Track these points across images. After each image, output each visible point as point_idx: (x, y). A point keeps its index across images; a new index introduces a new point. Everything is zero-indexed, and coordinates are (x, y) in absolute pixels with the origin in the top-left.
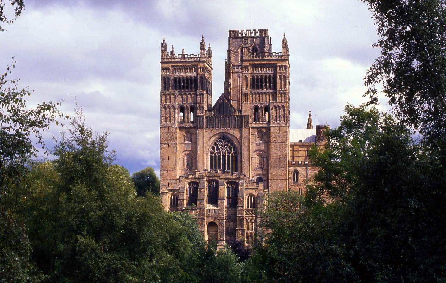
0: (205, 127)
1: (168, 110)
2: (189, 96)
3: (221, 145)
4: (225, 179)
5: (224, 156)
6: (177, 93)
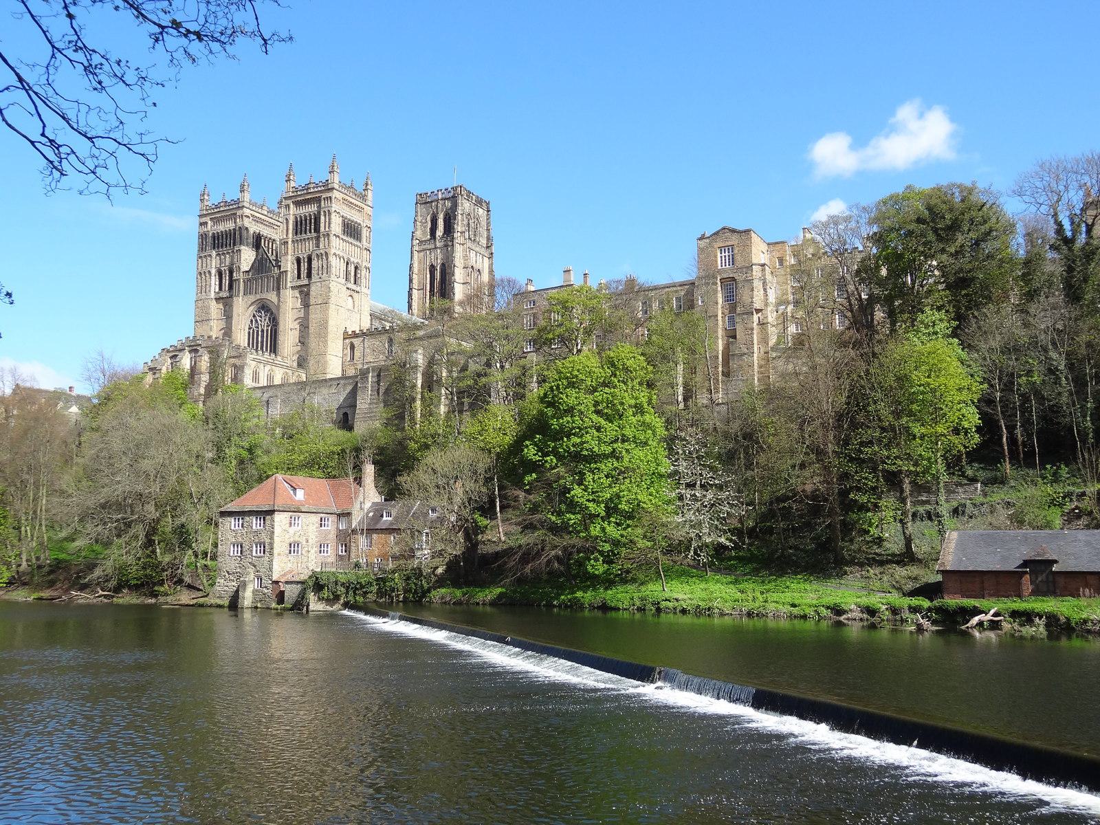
0: (241, 293)
1: (203, 276)
5: (263, 331)
6: (214, 253)
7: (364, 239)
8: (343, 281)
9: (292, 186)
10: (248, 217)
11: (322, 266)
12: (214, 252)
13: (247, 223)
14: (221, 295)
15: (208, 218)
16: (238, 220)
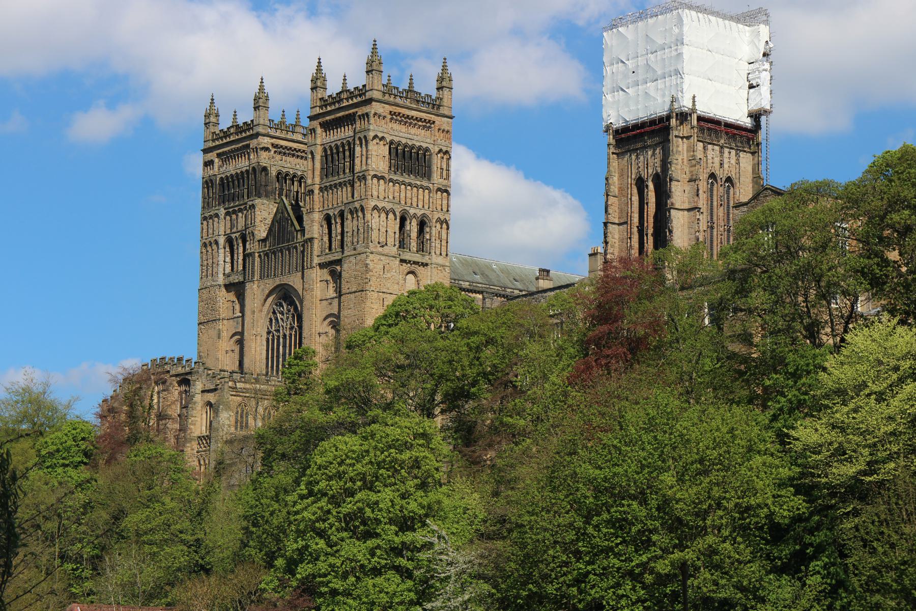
2: (240, 214)
4: (176, 376)
5: (285, 336)
6: (222, 212)
7: (436, 177)
8: (394, 250)
10: (266, 149)
11: (358, 229)
13: (264, 159)
16: (252, 157)
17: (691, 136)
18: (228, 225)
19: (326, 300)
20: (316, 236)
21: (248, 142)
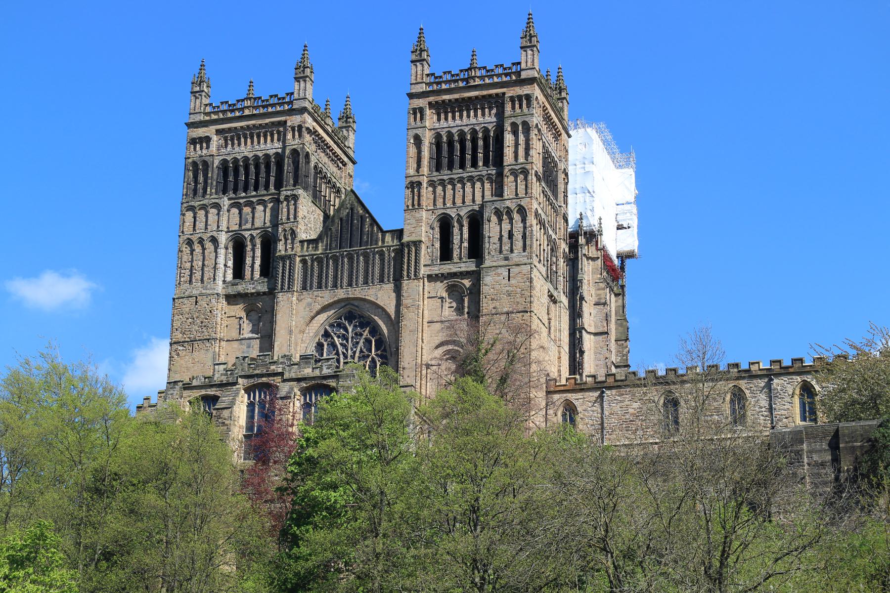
0: (297, 285)
1: (198, 249)
2: (260, 208)
3: (344, 335)
4: (298, 380)
6: (225, 202)
9: (427, 71)
12: (226, 199)
14: (241, 288)
15: (213, 128)
16: (289, 136)
17: (598, 258)
18: (237, 220)
19: (442, 322)
20: (423, 240)
21: (283, 119)
